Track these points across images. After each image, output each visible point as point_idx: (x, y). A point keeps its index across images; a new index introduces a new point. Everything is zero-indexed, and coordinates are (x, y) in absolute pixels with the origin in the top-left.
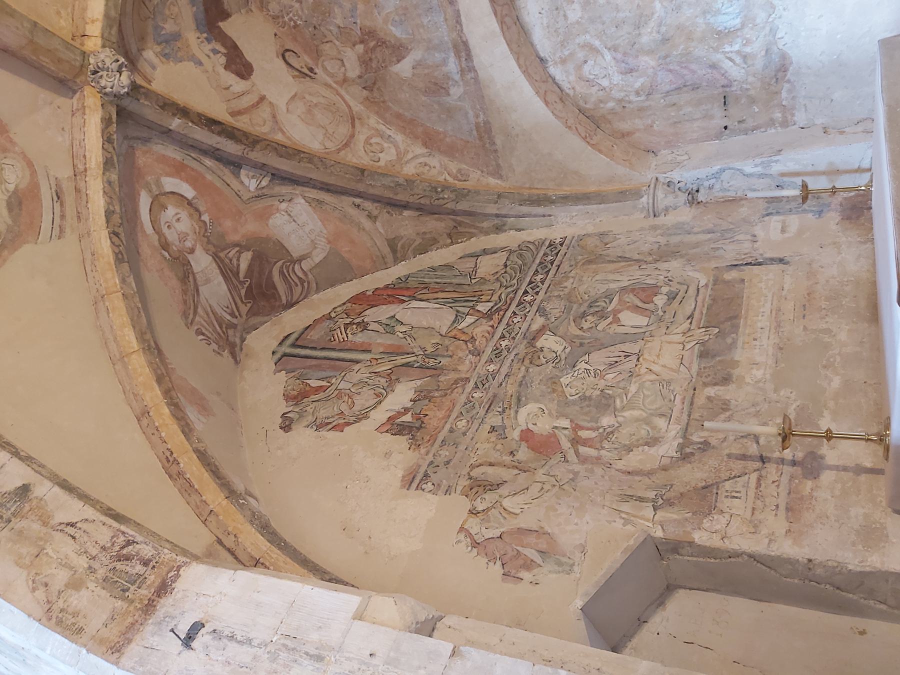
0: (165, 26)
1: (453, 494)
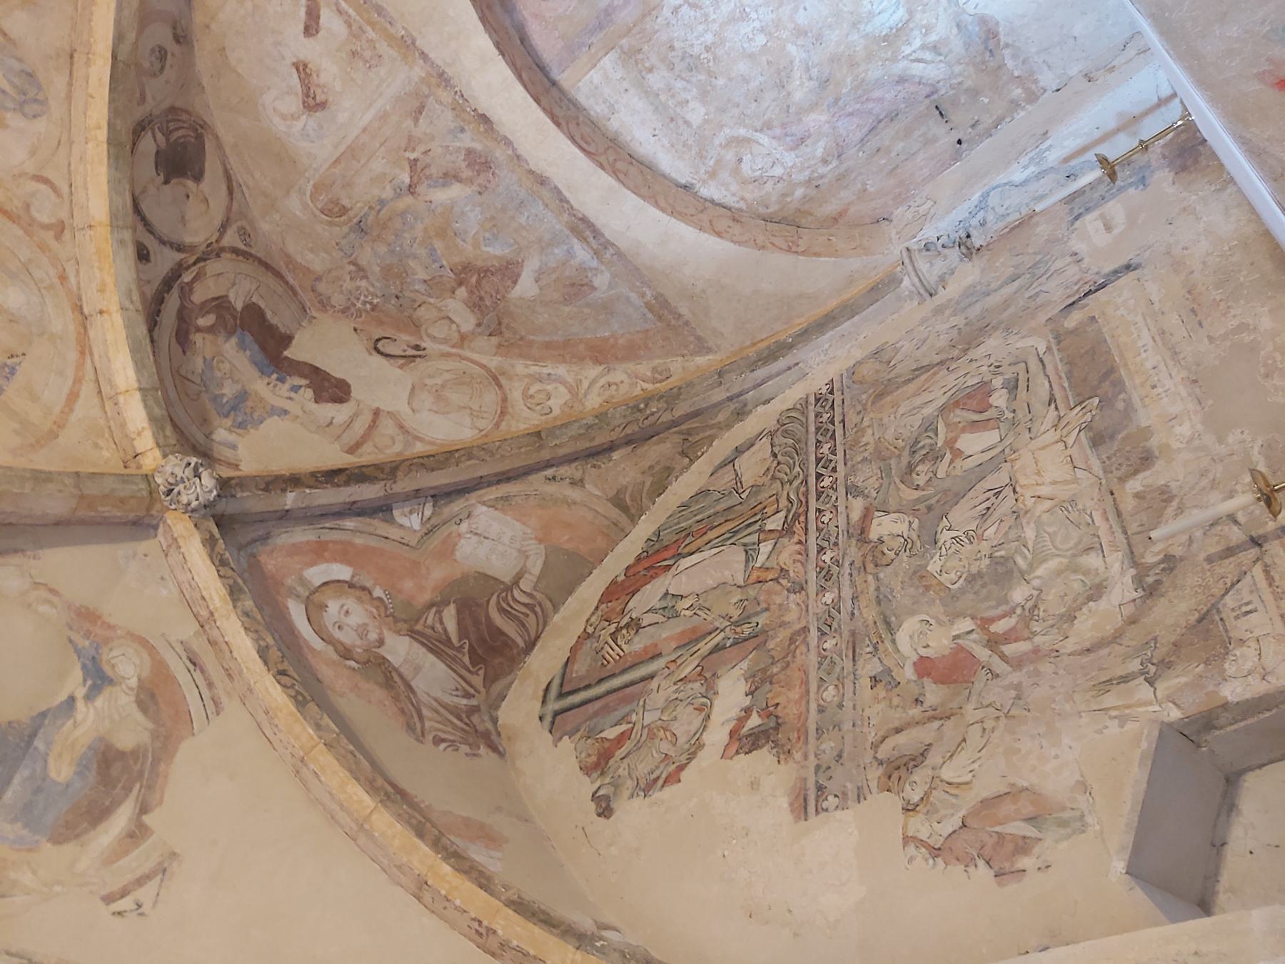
0: (224, 391)
1: (869, 797)
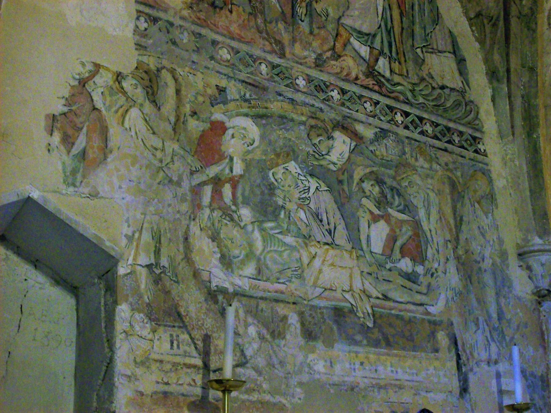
1: (137, 52)
